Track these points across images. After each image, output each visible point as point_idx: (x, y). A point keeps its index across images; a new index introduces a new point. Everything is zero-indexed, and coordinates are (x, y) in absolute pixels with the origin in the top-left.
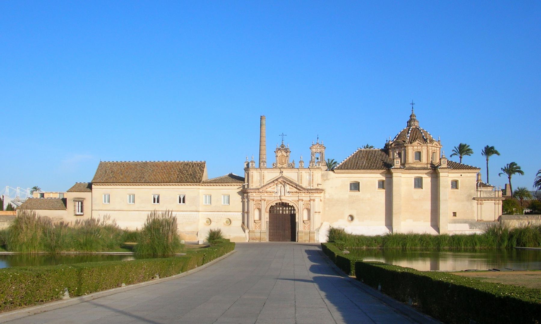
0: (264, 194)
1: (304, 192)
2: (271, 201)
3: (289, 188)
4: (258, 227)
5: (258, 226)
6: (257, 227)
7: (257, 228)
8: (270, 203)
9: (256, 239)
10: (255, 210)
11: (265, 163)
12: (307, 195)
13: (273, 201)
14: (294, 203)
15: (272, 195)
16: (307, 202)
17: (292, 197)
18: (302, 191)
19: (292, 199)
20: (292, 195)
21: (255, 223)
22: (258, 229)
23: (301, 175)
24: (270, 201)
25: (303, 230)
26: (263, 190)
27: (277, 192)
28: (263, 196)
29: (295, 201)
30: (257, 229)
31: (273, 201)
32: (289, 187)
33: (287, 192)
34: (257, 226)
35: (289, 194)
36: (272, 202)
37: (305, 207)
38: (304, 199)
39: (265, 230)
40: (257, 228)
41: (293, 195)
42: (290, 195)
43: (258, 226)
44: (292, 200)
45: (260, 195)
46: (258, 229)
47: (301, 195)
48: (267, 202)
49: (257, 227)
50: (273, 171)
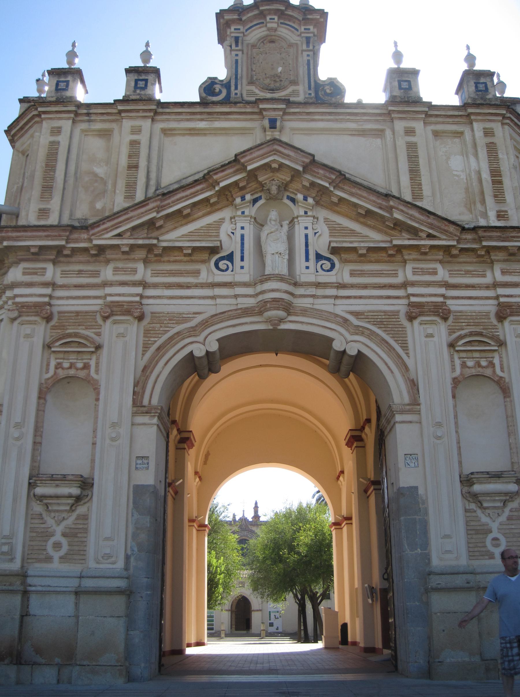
0: (131, 265)
1: (447, 249)
2: (178, 323)
3: (323, 228)
4: (64, 542)
5: (59, 530)
6: (58, 537)
7: (50, 550)
8: (171, 338)
9: (38, 651)
10: (49, 397)
11: (151, 77)
12: (468, 273)
13: (199, 318)
14: (371, 335)
15: (197, 273)
16: (477, 324)
17: (352, 286)
18: (430, 236)
19: (359, 306)
20: (353, 274)
21: (38, 508)
22: (63, 559)
23: (412, 147)
24: (181, 319)
25: (463, 561)
26: (119, 235)
27: (230, 257)
28: (123, 284)
29: (380, 324)
30: (49, 559)
31: (205, 324)
32: (326, 220)
33: (312, 256)
34: (48, 534)
35: (333, 266)
36: (194, 331)
37: (464, 365)
38: (453, 305)
39: (120, 564)
40: (57, 546)
41: (362, 274)
42: (331, 278)
43: (64, 535)
44: (357, 314)
45: (96, 274)
46: (63, 559)
47: (424, 272)
48: (147, 333)
49: (58, 537)
50: (202, 125)
